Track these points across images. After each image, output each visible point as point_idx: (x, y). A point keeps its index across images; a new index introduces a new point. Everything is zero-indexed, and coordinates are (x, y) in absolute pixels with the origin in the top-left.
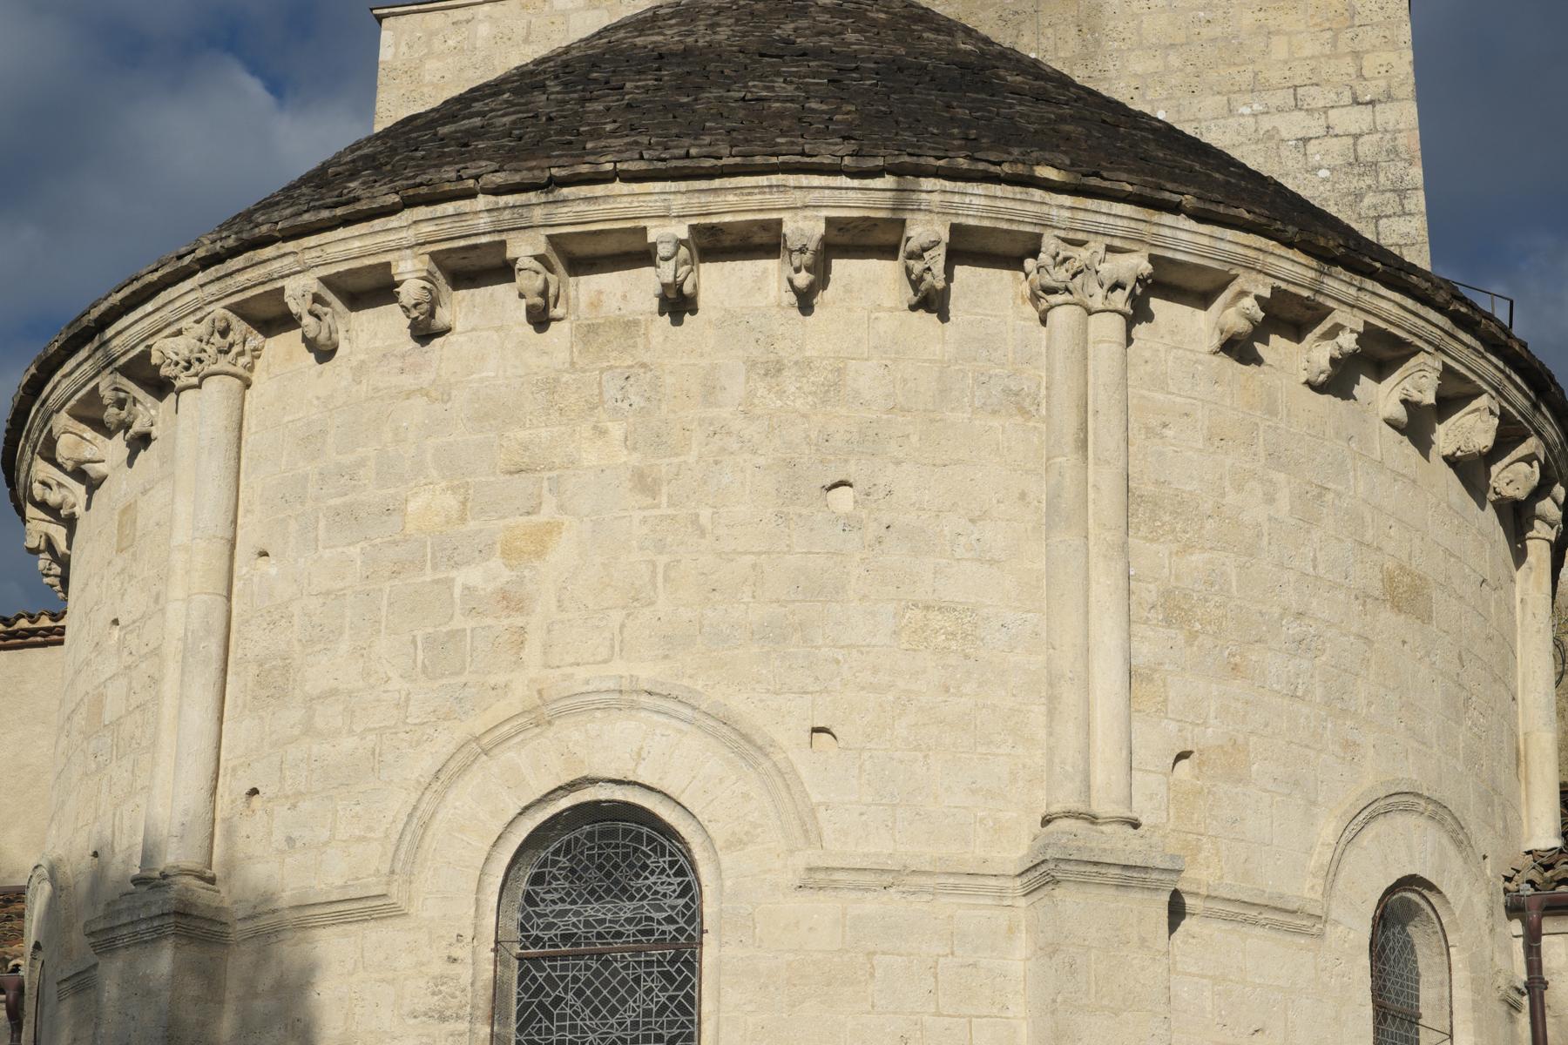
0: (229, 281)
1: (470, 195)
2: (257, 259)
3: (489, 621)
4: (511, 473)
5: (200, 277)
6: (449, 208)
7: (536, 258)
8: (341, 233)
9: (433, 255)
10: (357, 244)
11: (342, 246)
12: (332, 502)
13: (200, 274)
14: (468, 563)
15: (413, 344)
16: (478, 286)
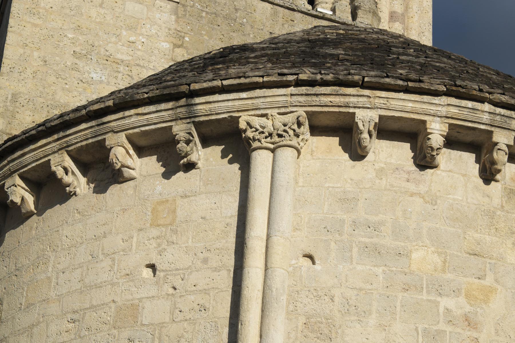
0: (314, 98)
1: (482, 101)
2: (341, 92)
3: (459, 330)
4: (470, 254)
5: (292, 90)
6: (470, 104)
7: (508, 146)
8: (401, 95)
9: (450, 125)
10: (410, 104)
11: (401, 103)
12: (363, 240)
13: (292, 88)
14: (447, 296)
15: (414, 168)
16: (453, 149)
